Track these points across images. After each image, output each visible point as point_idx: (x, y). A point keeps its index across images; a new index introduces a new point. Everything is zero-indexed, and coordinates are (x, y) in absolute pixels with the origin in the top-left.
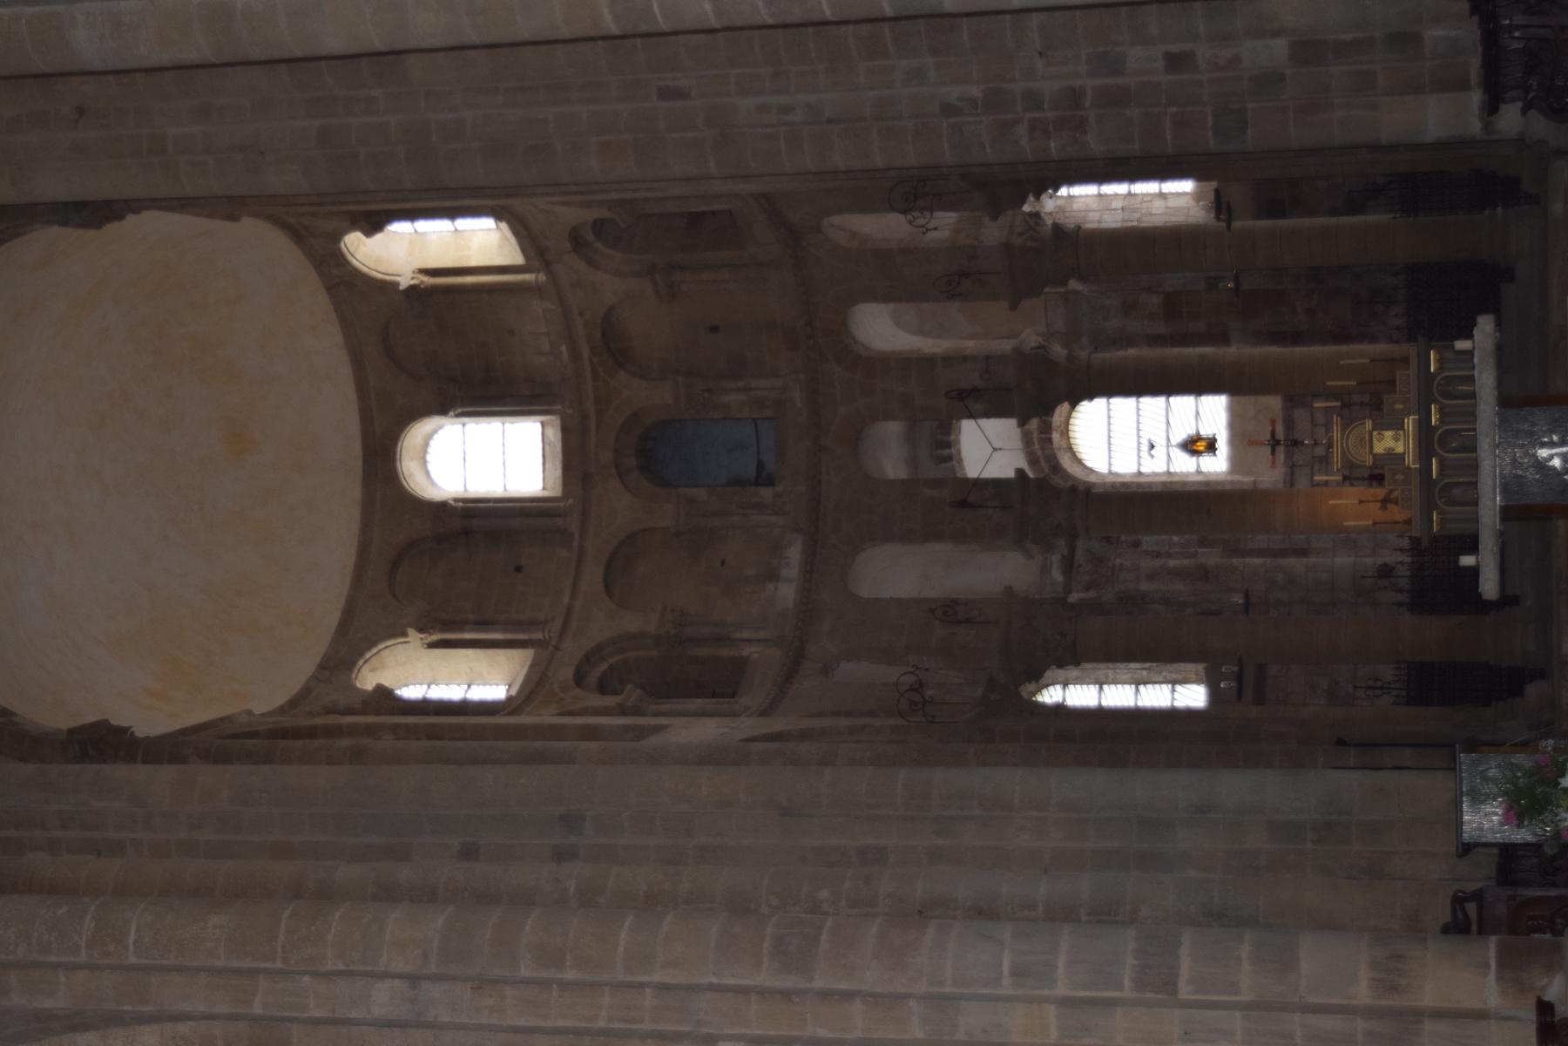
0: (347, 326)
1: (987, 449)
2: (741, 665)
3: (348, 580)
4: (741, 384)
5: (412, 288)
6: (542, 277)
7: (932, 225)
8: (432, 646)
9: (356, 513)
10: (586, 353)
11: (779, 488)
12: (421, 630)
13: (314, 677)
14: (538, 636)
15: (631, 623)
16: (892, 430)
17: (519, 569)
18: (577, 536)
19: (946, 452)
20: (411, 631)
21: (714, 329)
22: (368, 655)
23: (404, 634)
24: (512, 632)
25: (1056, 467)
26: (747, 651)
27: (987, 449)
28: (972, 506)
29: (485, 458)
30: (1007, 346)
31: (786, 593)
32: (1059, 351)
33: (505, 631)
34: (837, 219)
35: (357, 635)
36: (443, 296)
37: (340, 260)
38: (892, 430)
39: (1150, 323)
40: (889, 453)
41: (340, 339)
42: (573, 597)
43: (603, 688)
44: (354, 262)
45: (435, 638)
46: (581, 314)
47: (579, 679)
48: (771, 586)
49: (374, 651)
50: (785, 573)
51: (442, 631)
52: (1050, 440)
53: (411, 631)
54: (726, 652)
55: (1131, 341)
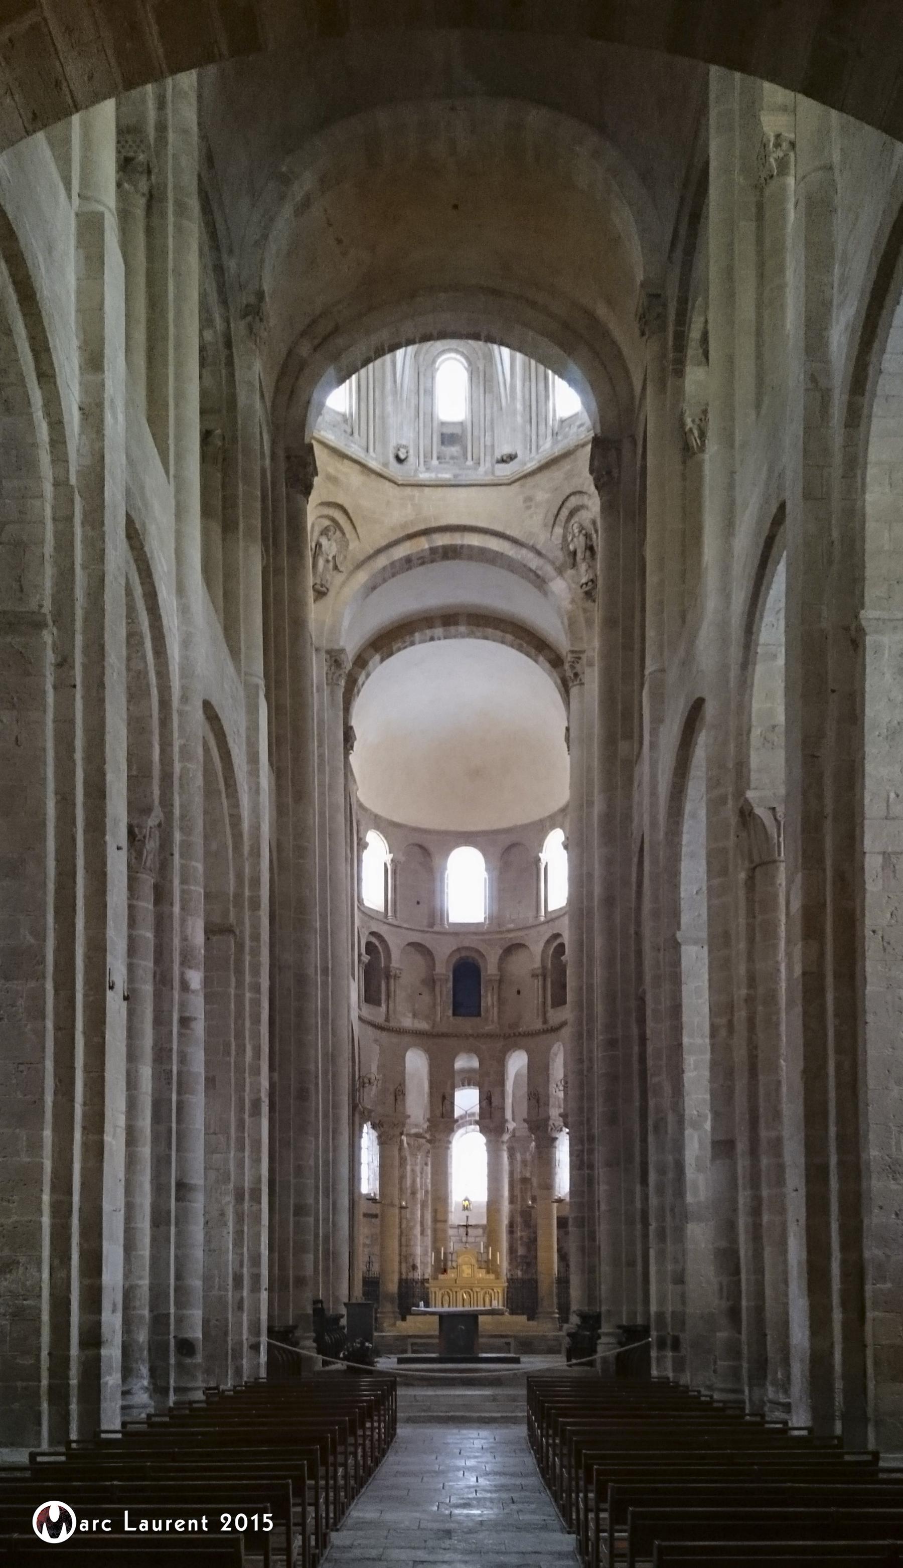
9: (443, 828)
11: (451, 1018)
16: (475, 1063)
38: (475, 1063)
39: (524, 1182)
40: (464, 1062)
41: (519, 823)
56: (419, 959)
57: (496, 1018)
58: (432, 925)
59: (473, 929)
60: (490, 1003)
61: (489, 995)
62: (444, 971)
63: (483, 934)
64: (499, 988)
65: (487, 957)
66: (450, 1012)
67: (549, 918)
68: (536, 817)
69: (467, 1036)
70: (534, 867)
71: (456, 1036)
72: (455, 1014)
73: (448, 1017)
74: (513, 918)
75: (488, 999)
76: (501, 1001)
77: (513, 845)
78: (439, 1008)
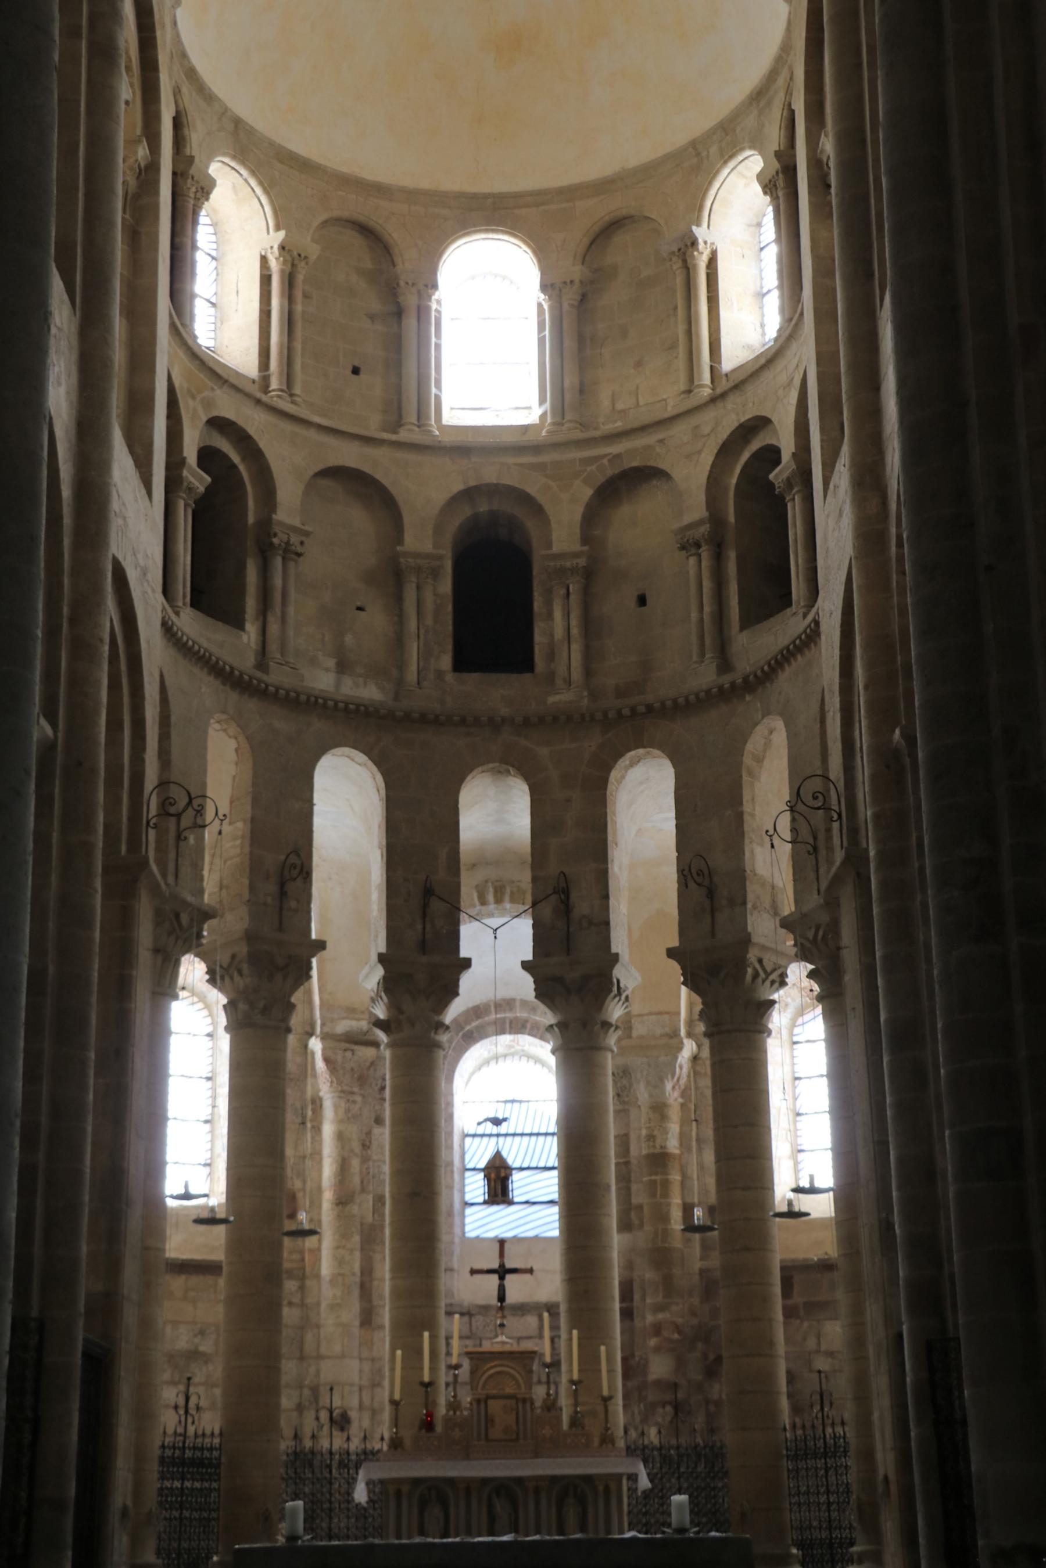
0: (647, 171)
1: (497, 948)
2: (237, 622)
3: (344, 169)
4: (575, 631)
5: (694, 243)
6: (706, 392)
7: (776, 841)
8: (264, 259)
9: (425, 184)
10: (613, 449)
11: (450, 677)
12: (282, 248)
13: (225, 111)
14: (274, 384)
15: (289, 493)
17: (356, 371)
18: (394, 437)
19: (491, 898)
20: (282, 234)
21: (642, 601)
22: (253, 182)
23: (278, 228)
24: (280, 353)
25: (471, 1038)
26: (251, 628)
27: (497, 948)
28: (425, 906)
29: (489, 339)
30: (620, 942)
31: (322, 680)
32: (616, 1012)
33: (281, 345)
34: (780, 738)
35: (278, 169)
36: (683, 275)
37: (728, 154)
41: (633, 162)
42: (320, 427)
43: (207, 456)
44: (725, 171)
45: (274, 265)
46: (661, 441)
47: (218, 424)
48: (331, 663)
49: (258, 190)
50: (348, 681)
51: (282, 272)
52: (502, 1032)
53: (282, 234)
54: (251, 604)
55: (622, 1113)
56: (359, 520)
57: (577, 674)
58: (397, 423)
59: (509, 439)
60: (559, 633)
61: (558, 614)
62: (428, 547)
63: (537, 449)
64: (587, 592)
65: (548, 508)
66: (446, 661)
67: (724, 385)
68: (679, 139)
69: (495, 724)
70: (677, 264)
71: (463, 721)
72: (461, 664)
73: (440, 675)
74: (620, 406)
75: (555, 624)
76: (592, 628)
77: (611, 229)
78: (413, 649)
